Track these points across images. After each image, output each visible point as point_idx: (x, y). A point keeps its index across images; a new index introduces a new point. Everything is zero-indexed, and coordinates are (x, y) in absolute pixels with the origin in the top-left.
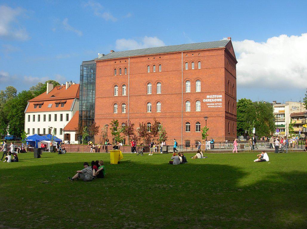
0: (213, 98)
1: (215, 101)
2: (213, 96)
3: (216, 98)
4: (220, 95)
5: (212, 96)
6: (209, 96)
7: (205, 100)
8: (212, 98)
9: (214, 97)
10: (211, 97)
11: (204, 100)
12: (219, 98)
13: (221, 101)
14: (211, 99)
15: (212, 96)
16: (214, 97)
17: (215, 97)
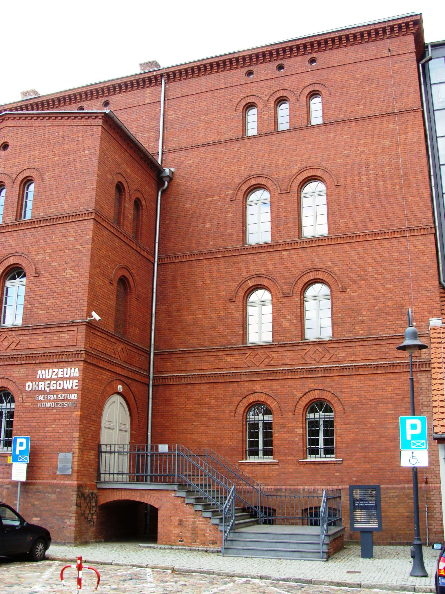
0: (54, 379)
1: (58, 388)
2: (56, 370)
3: (64, 379)
4: (73, 370)
5: (53, 372)
6: (43, 371)
7: (30, 383)
8: (51, 379)
9: (57, 374)
10: (50, 377)
11: (27, 384)
12: (70, 378)
13: (74, 387)
14: (47, 383)
15: (53, 372)
16: (57, 374)
17: (60, 376)
